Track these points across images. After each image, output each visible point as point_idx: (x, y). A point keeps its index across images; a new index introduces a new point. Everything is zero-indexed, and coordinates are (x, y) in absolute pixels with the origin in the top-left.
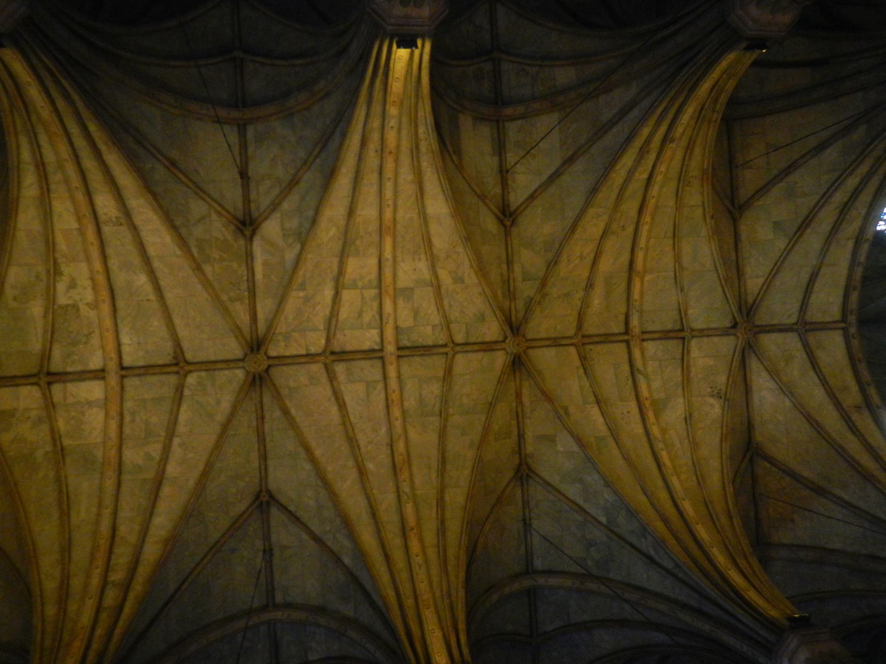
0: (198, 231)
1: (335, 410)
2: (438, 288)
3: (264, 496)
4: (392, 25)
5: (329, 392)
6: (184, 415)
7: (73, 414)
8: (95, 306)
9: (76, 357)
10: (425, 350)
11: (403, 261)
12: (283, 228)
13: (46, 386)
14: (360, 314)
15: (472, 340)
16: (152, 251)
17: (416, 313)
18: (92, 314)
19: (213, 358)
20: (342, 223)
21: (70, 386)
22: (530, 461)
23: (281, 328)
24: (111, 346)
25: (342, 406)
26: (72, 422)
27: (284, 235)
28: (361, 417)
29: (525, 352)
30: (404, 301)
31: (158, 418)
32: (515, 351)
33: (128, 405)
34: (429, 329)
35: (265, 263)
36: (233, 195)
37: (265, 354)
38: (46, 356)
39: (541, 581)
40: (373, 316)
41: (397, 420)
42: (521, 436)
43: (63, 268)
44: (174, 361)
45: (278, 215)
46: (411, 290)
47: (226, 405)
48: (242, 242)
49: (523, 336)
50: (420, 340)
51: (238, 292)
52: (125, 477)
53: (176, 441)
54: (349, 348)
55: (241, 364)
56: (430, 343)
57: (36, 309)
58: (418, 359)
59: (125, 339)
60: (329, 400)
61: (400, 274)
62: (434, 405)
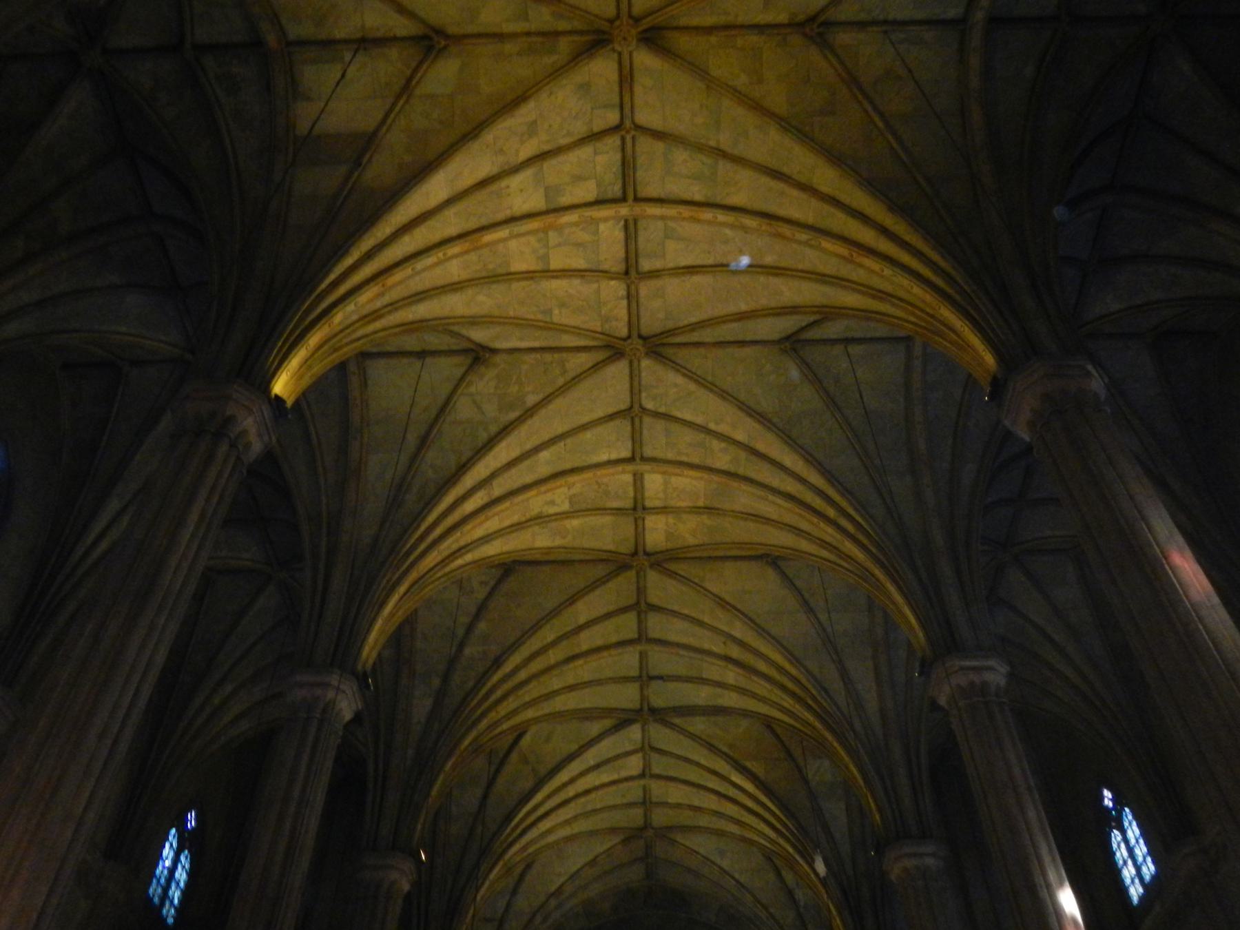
1: (696, 279)
3: (786, 347)
4: (270, 438)
5: (675, 281)
10: (627, 167)
11: (511, 208)
14: (578, 245)
15: (616, 100)
17: (578, 179)
18: (578, 485)
19: (627, 386)
21: (647, 494)
22: (801, 17)
23: (597, 325)
25: (691, 270)
28: (709, 253)
29: (637, 20)
30: (563, 196)
31: (688, 436)
32: (635, 42)
33: (670, 455)
34: (599, 159)
36: (446, 369)
37: (625, 340)
39: (979, 16)
40: (583, 229)
41: (717, 218)
42: (759, 28)
44: (629, 419)
46: (547, 189)
47: (680, 380)
48: (498, 359)
49: (611, 21)
50: (614, 170)
51: (554, 365)
52: (741, 471)
53: (712, 426)
54: (622, 254)
55: (635, 364)
56: (618, 156)
58: (639, 173)
59: (604, 457)
60: (684, 281)
61: (526, 207)
62: (703, 164)
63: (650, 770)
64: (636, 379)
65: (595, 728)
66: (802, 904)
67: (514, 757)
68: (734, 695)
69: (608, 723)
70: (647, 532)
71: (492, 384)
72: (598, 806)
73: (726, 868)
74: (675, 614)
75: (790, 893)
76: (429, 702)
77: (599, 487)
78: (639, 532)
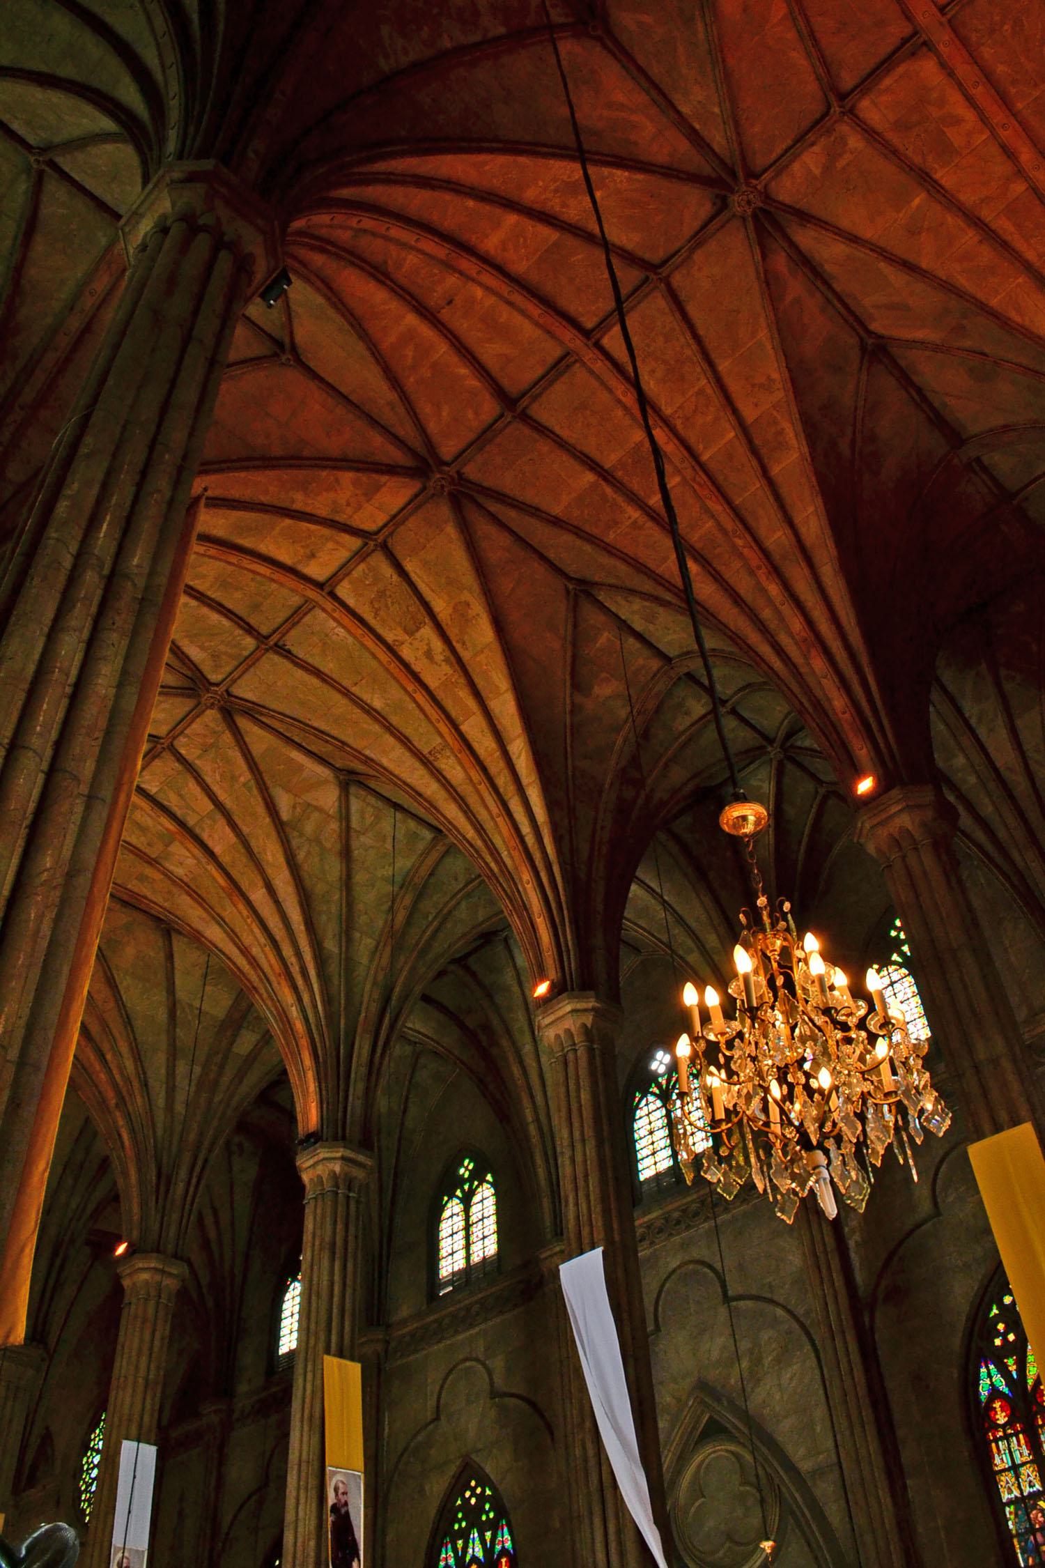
2: (152, 862)
12: (318, 809)
14: (181, 796)
20: (269, 871)
27: (309, 805)
35: (301, 768)
43: (447, 669)
45: (331, 812)
46: (167, 845)
65: (829, 252)
68: (530, 195)
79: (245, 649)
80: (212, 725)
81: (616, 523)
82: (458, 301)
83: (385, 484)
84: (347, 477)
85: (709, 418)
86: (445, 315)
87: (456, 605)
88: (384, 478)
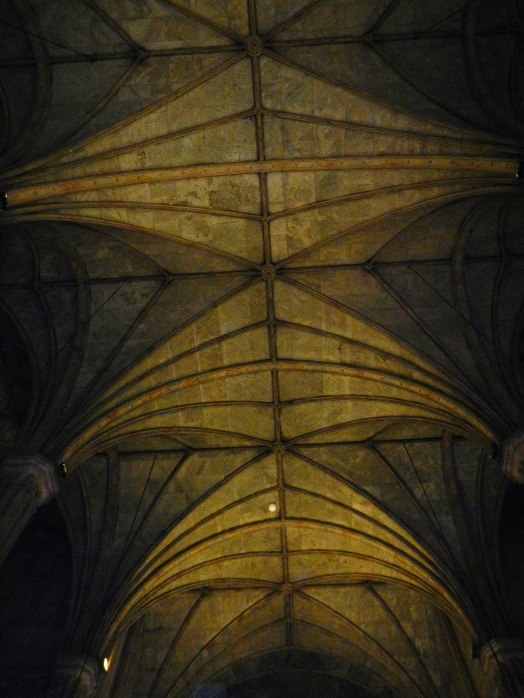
0: (144, 94)
6: (297, 109)
7: (292, 196)
8: (210, 178)
9: (249, 195)
12: (135, 19)
13: (270, 216)
16: (164, 131)
18: (216, 181)
21: (270, 200)
24: (241, 168)
26: (298, 197)
27: (142, 18)
38: (248, 217)
43: (182, 199)
44: (253, 119)
45: (124, 23)
48: (152, 60)
51: (194, 63)
52: (343, 151)
53: (317, 114)
57: (213, 221)
63: (285, 512)
64: (257, 76)
65: (238, 460)
66: (421, 651)
67: (171, 487)
68: (350, 404)
69: (249, 455)
70: (272, 239)
71: (148, 78)
72: (243, 551)
73: (353, 620)
74: (300, 327)
75: (410, 642)
76: (90, 376)
77: (233, 188)
78: (267, 239)
79: (266, 97)
80: (238, 22)
81: (198, 332)
82: (337, 351)
83: (288, 249)
84: (307, 243)
85: (214, 395)
86: (337, 343)
87: (210, 229)
88: (291, 252)
